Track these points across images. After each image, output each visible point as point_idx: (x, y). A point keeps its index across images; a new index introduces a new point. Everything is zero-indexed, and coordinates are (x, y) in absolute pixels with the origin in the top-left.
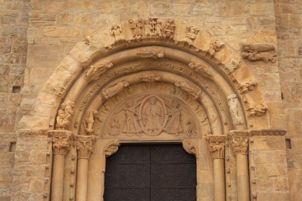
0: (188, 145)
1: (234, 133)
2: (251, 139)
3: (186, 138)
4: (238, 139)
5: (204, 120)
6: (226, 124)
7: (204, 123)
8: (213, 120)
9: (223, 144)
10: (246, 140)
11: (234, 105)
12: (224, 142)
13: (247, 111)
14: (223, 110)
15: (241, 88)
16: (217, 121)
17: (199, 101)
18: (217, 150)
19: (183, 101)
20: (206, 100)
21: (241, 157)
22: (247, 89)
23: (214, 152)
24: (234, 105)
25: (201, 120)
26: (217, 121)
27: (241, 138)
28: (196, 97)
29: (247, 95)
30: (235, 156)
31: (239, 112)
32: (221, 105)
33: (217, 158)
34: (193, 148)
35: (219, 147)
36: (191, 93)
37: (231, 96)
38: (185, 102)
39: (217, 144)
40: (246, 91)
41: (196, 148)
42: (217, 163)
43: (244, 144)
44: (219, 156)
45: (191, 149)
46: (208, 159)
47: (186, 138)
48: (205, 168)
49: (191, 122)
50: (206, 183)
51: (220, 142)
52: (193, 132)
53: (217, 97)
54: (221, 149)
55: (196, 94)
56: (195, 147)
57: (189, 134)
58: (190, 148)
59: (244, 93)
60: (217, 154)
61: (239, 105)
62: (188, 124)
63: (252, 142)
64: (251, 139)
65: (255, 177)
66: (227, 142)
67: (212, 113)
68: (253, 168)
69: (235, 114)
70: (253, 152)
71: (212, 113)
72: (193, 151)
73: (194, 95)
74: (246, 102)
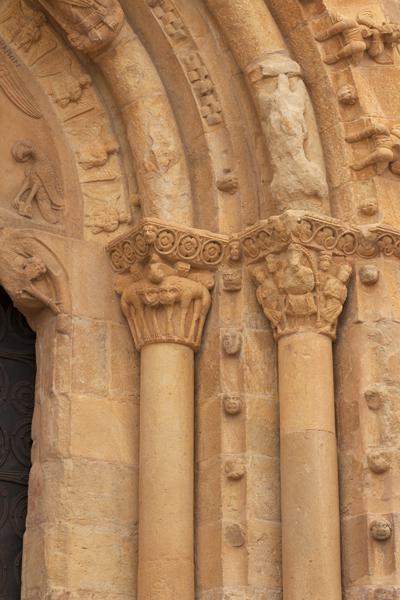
0: (20, 260)
1: (306, 227)
2: (372, 268)
3: (14, 223)
4: (312, 255)
5: (104, 157)
6: (227, 189)
7: (99, 174)
8: (164, 160)
9: (207, 278)
10: (345, 271)
11: (289, 103)
12: (213, 270)
13: (351, 141)
14: (215, 123)
15: (339, 35)
16: (177, 167)
17: (95, 63)
18: (177, 302)
19: (13, 46)
20: (135, 67)
21: (309, 347)
22: (363, 45)
23: (160, 307)
24: (289, 103)
25: (86, 157)
26: (177, 167)
27: (327, 254)
28: (99, 34)
29: (358, 72)
30: (272, 339)
31: (310, 141)
32: (210, 98)
33: (170, 341)
34: (46, 276)
35: (189, 286)
36: (75, 11)
37: (277, 61)
38: (19, 53)
39: (181, 274)
40: (359, 51)
41: (61, 280)
42: (167, 367)
43: (335, 286)
44: (181, 330)
45: (34, 280)
46: (108, 344)
47: (14, 223)
48: (97, 383)
49: (41, 155)
50: (96, 454)
51: (195, 268)
52: (45, 205)
53: (202, 57)
54: (196, 298)
55: (101, 22)
56: (57, 273)
57: (25, 207)
58: (32, 271)
59: (346, 59)
60: (179, 324)
61: (311, 112)
62: (17, 160)
63: (371, 284)
64: (372, 268)
65: (382, 440)
66: (227, 272)
67: (157, 129)
68: (375, 401)
69: (295, 143)
70: (370, 325)
71: (157, 129)
72: (41, 291)
73: (87, 21)
74: (350, 103)
